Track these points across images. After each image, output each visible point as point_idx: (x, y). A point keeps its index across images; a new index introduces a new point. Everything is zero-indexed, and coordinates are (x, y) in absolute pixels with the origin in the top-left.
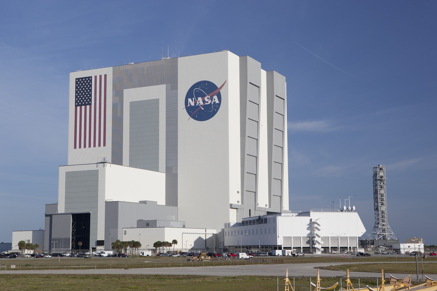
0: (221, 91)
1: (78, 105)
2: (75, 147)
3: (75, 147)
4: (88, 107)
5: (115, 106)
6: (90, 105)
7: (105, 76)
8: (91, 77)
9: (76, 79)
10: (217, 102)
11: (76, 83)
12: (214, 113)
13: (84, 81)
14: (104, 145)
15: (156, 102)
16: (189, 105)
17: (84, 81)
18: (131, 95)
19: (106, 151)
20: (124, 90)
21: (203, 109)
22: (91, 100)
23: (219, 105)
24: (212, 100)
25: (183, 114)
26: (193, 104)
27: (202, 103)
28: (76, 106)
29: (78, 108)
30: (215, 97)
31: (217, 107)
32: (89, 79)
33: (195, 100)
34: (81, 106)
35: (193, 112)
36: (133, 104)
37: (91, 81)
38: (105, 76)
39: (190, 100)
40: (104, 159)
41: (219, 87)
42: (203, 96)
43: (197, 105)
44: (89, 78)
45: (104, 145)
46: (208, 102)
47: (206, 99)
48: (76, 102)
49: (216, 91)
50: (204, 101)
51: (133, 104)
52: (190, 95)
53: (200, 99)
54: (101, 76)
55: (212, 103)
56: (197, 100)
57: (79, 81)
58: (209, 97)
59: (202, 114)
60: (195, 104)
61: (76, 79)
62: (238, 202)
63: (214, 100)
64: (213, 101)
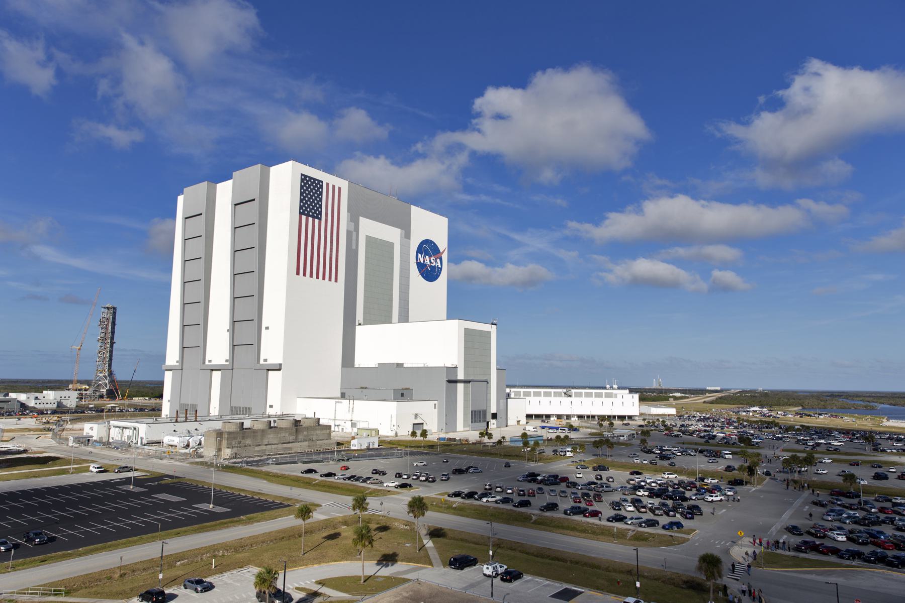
2: (298, 273)
3: (298, 273)
4: (317, 221)
5: (349, 233)
6: (320, 219)
7: (340, 189)
9: (302, 175)
11: (302, 180)
12: (438, 277)
13: (312, 183)
14: (336, 280)
17: (312, 183)
20: (361, 218)
22: (320, 213)
29: (304, 217)
30: (438, 260)
34: (308, 215)
37: (321, 187)
38: (340, 189)
42: (430, 256)
44: (320, 181)
45: (336, 280)
48: (301, 207)
49: (438, 255)
52: (419, 250)
54: (334, 186)
59: (430, 274)
61: (302, 175)
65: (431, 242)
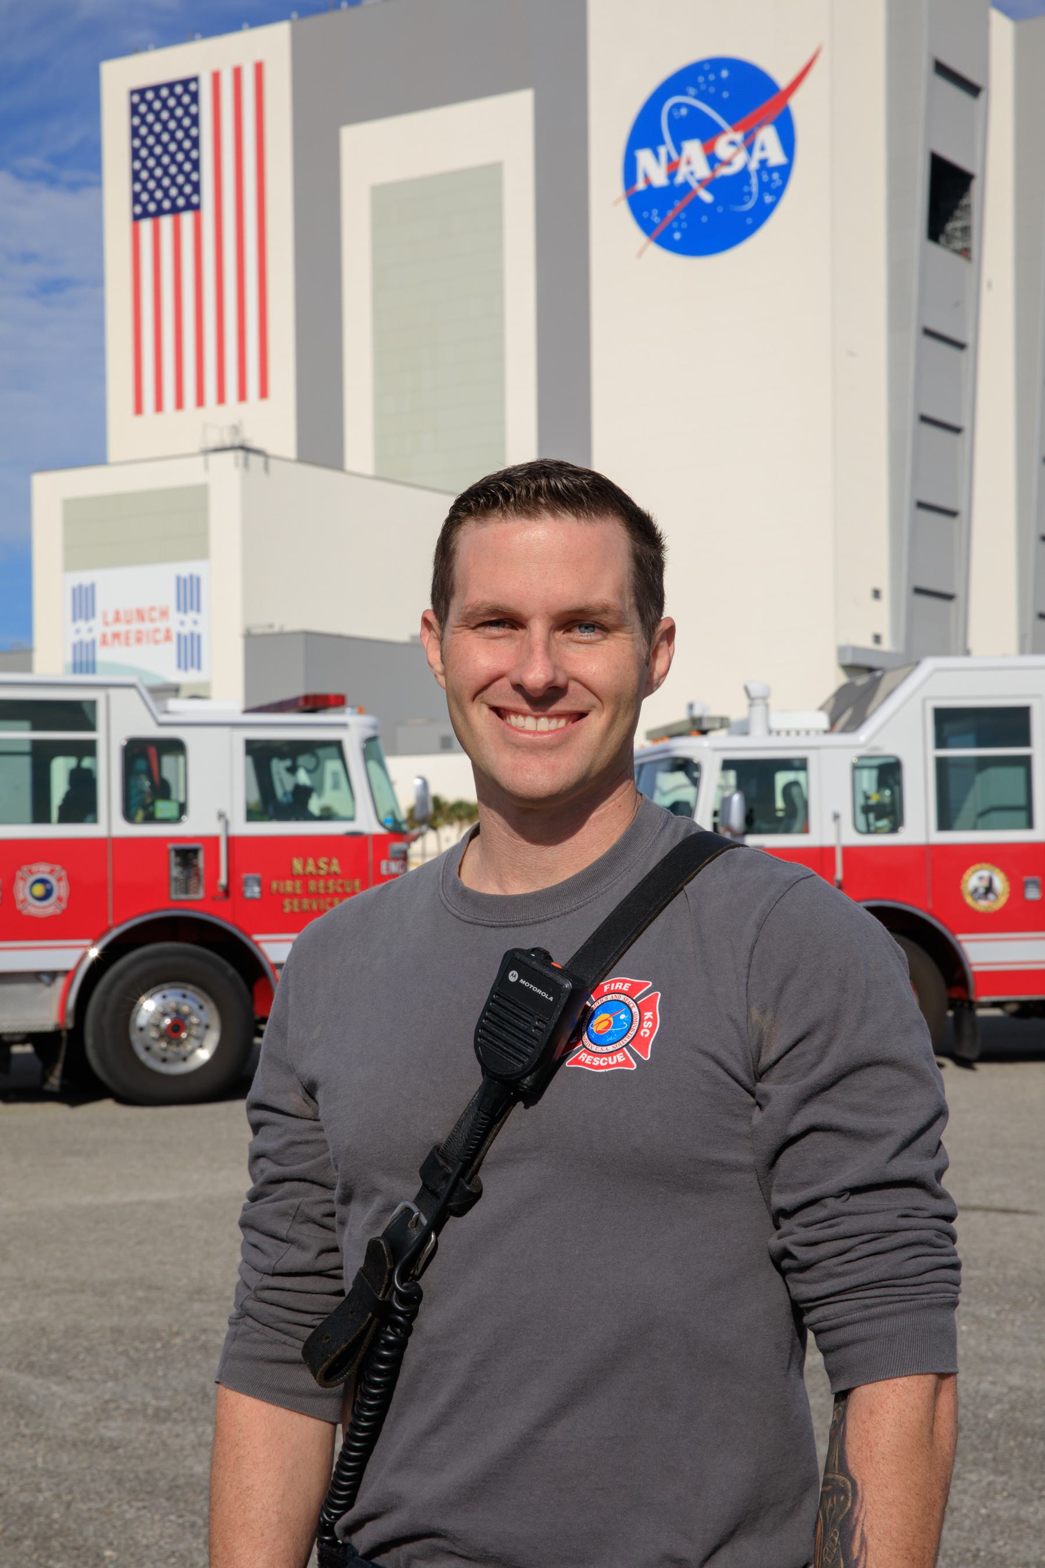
0: (795, 103)
1: (145, 214)
2: (138, 409)
3: (138, 409)
4: (187, 219)
6: (196, 208)
7: (259, 68)
8: (195, 79)
10: (776, 156)
11: (134, 110)
14: (264, 393)
15: (489, 177)
16: (641, 185)
18: (376, 152)
19: (273, 421)
21: (707, 197)
23: (785, 171)
24: (750, 150)
25: (612, 226)
26: (659, 179)
27: (702, 170)
28: (136, 218)
30: (768, 136)
31: (775, 181)
32: (186, 90)
33: (669, 158)
35: (662, 215)
36: (383, 197)
37: (195, 98)
38: (259, 68)
39: (644, 157)
40: (236, 429)
41: (783, 81)
43: (679, 179)
44: (185, 83)
45: (264, 393)
46: (728, 163)
47: (723, 148)
48: (136, 198)
50: (713, 160)
51: (383, 197)
53: (693, 149)
55: (754, 165)
56: (679, 150)
57: (143, 100)
58: (738, 137)
59: (705, 222)
60: (672, 174)
61: (133, 92)
62: (877, 639)
63: (763, 148)
64: (758, 155)
65: (717, 64)
